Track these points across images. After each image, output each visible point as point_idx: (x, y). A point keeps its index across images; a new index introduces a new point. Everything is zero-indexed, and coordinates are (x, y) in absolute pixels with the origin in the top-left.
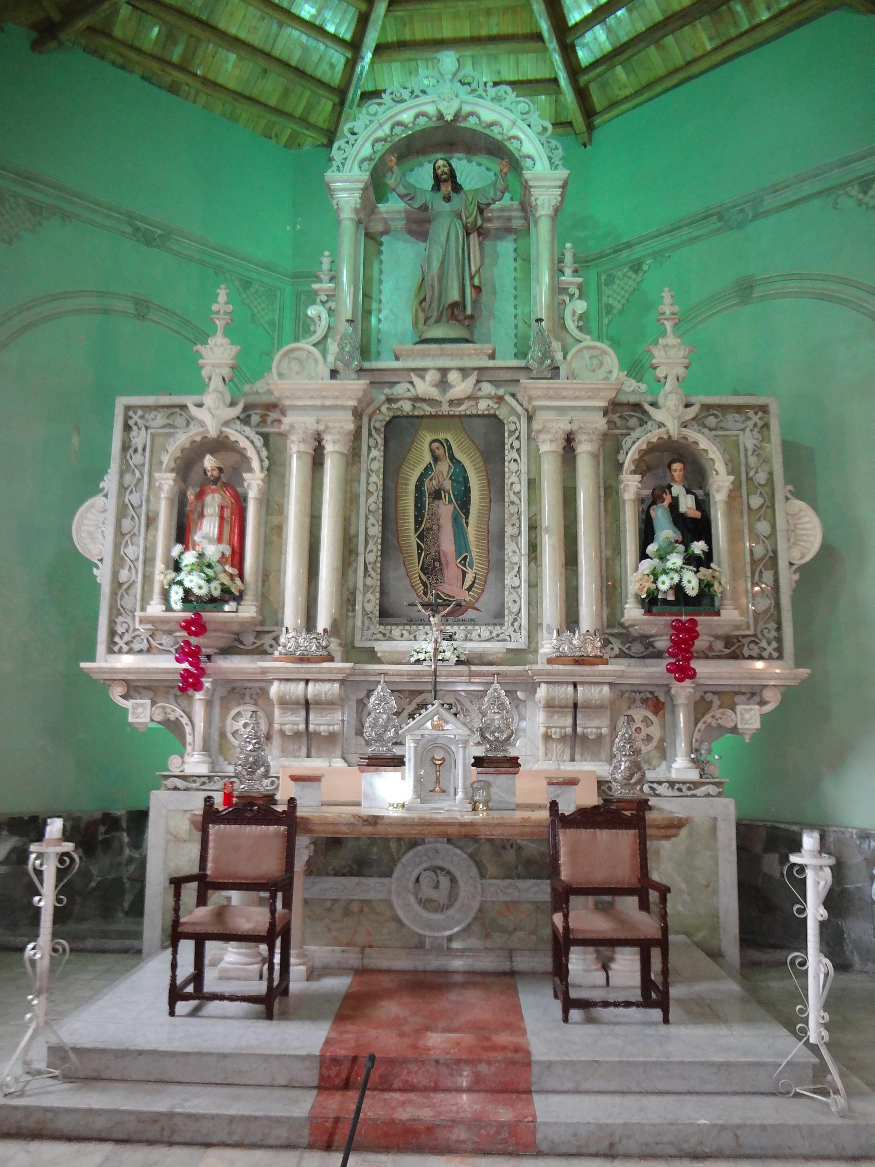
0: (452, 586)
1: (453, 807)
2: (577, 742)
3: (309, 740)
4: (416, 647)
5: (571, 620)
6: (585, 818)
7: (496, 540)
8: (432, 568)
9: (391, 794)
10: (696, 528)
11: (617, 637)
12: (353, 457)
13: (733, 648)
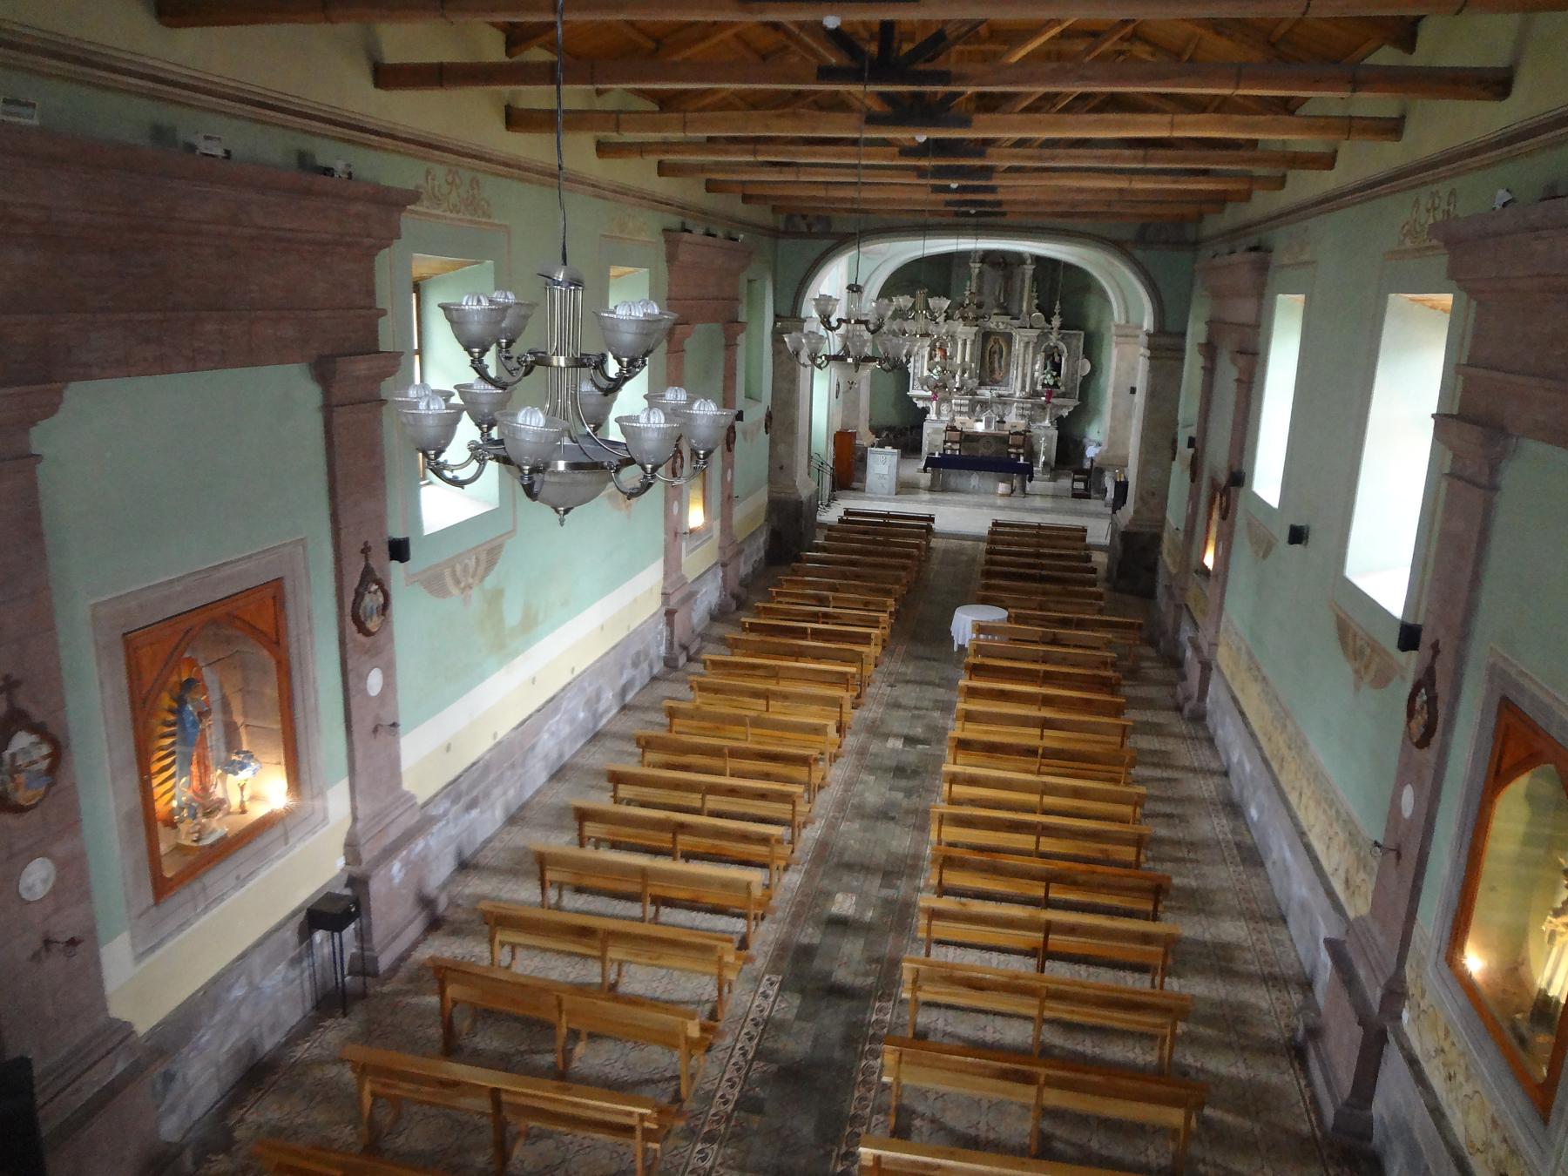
0: (997, 376)
1: (992, 430)
2: (1023, 416)
3: (961, 413)
4: (986, 393)
5: (1023, 388)
6: (1017, 433)
7: (1008, 365)
8: (992, 371)
9: (980, 427)
10: (1057, 367)
11: (1035, 394)
12: (973, 342)
13: (1063, 395)
